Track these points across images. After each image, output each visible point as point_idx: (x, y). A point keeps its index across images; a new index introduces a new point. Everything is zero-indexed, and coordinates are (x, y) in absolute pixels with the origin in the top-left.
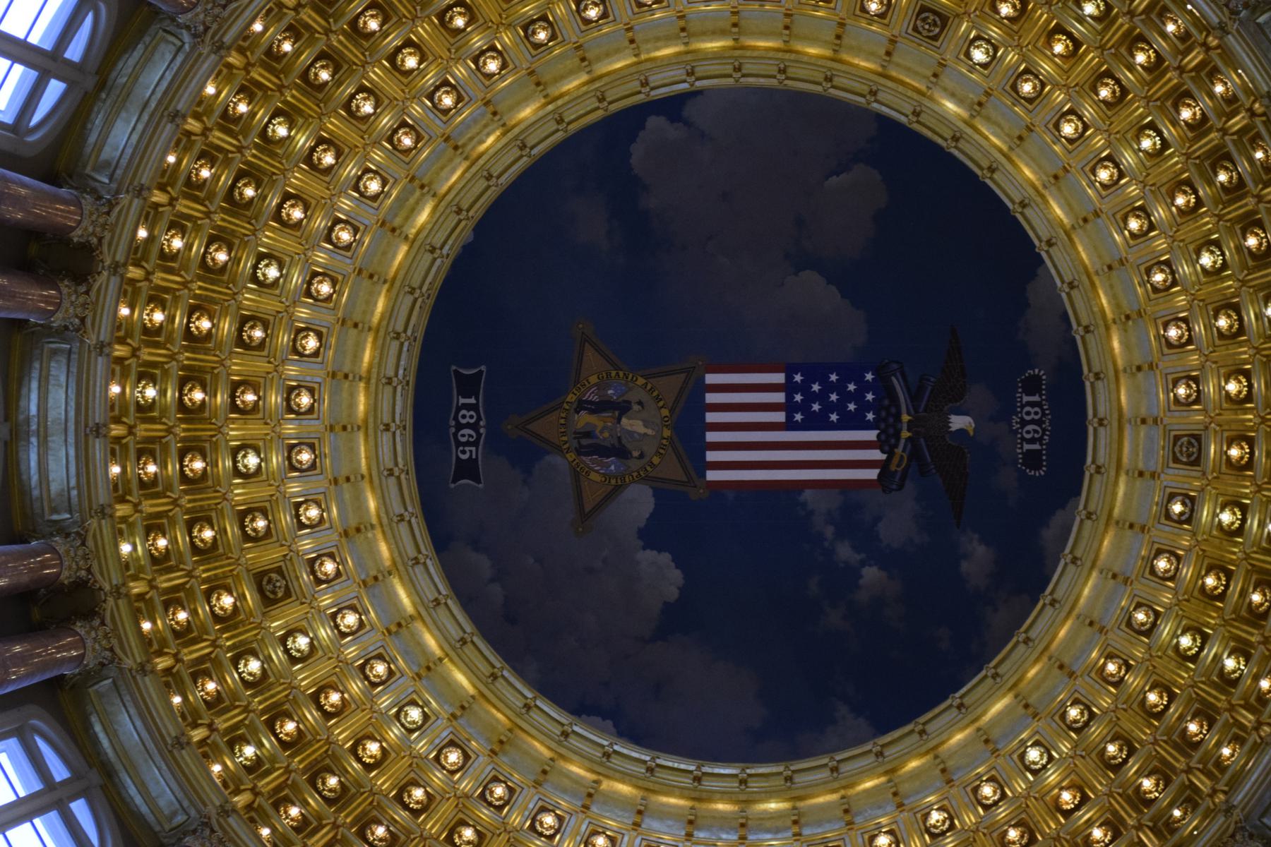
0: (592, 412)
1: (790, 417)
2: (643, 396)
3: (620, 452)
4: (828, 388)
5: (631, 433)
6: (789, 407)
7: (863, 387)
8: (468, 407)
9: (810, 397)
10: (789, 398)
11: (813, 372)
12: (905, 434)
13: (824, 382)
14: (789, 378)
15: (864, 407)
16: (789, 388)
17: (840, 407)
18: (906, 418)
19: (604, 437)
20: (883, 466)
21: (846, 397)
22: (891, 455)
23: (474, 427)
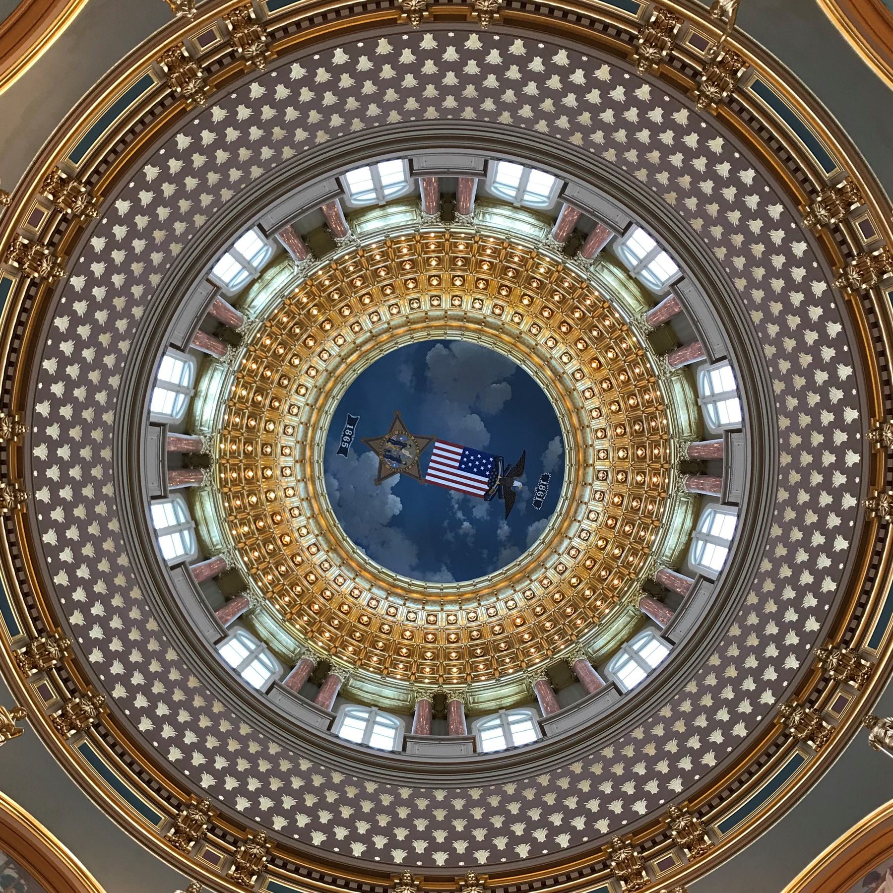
1: (460, 466)
2: (412, 443)
3: (399, 461)
4: (476, 459)
5: (404, 455)
6: (461, 462)
7: (488, 462)
8: (350, 429)
9: (469, 461)
10: (462, 458)
11: (473, 452)
12: (498, 483)
13: (476, 457)
14: (464, 452)
15: (486, 469)
18: (499, 477)
19: (394, 454)
20: (487, 491)
21: (481, 464)
22: (491, 488)
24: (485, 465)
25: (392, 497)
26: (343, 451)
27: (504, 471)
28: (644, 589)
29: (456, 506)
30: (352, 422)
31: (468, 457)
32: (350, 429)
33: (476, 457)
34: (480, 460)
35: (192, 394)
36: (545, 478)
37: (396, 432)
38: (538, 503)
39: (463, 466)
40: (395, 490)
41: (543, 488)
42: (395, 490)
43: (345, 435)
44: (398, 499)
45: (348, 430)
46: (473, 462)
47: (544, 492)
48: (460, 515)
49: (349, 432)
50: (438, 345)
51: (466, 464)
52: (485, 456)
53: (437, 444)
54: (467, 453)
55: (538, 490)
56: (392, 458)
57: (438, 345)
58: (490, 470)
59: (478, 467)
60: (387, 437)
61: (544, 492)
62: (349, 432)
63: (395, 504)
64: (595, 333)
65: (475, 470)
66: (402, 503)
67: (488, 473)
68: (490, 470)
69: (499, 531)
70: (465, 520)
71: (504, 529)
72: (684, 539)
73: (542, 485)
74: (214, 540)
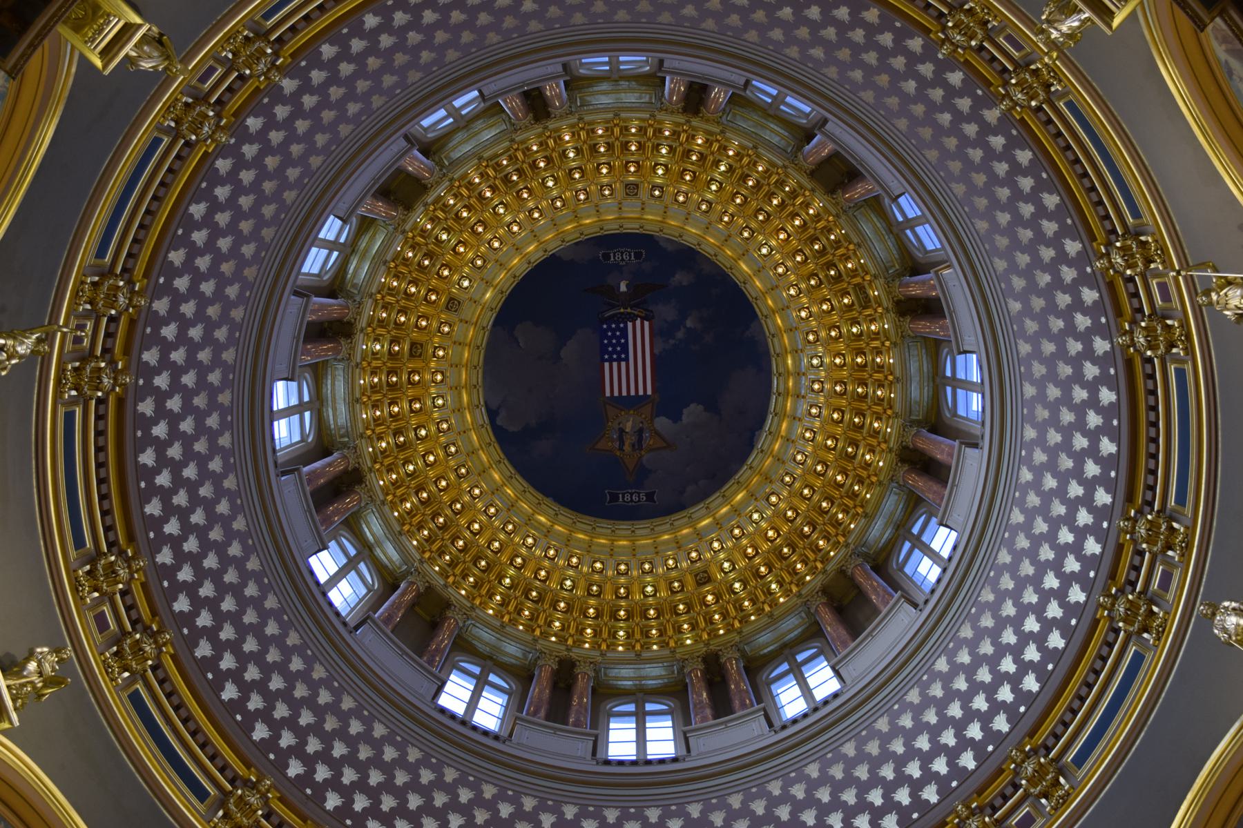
0: (624, 445)
1: (623, 360)
3: (641, 431)
4: (610, 344)
5: (633, 427)
7: (610, 328)
8: (623, 497)
9: (615, 351)
10: (615, 360)
11: (603, 349)
12: (629, 310)
13: (607, 346)
14: (607, 360)
15: (618, 328)
16: (611, 361)
17: (618, 338)
18: (622, 310)
20: (643, 319)
21: (614, 336)
23: (632, 494)
24: (614, 331)
25: (686, 418)
26: (650, 497)
27: (613, 307)
28: (696, 112)
29: (672, 342)
30: (614, 498)
31: (610, 354)
32: (623, 497)
33: (607, 346)
34: (610, 339)
35: (640, 695)
36: (606, 257)
37: (610, 444)
38: (638, 256)
39: (623, 356)
40: (676, 417)
41: (618, 257)
42: (676, 417)
43: (632, 501)
44: (685, 411)
45: (625, 498)
46: (614, 346)
47: (622, 253)
48: (680, 335)
49: (627, 498)
50: (499, 422)
51: (619, 354)
52: (603, 334)
53: (608, 394)
54: (606, 357)
55: (623, 260)
56: (640, 440)
57: (499, 422)
58: (618, 324)
59: (618, 338)
60: (618, 453)
61: (622, 253)
62: (627, 498)
63: (692, 412)
64: (427, 262)
65: (623, 341)
66: (687, 406)
67: (622, 325)
68: (618, 324)
69: (685, 283)
70: (685, 327)
71: (681, 278)
72: (624, 84)
73: (615, 257)
74: (797, 622)
